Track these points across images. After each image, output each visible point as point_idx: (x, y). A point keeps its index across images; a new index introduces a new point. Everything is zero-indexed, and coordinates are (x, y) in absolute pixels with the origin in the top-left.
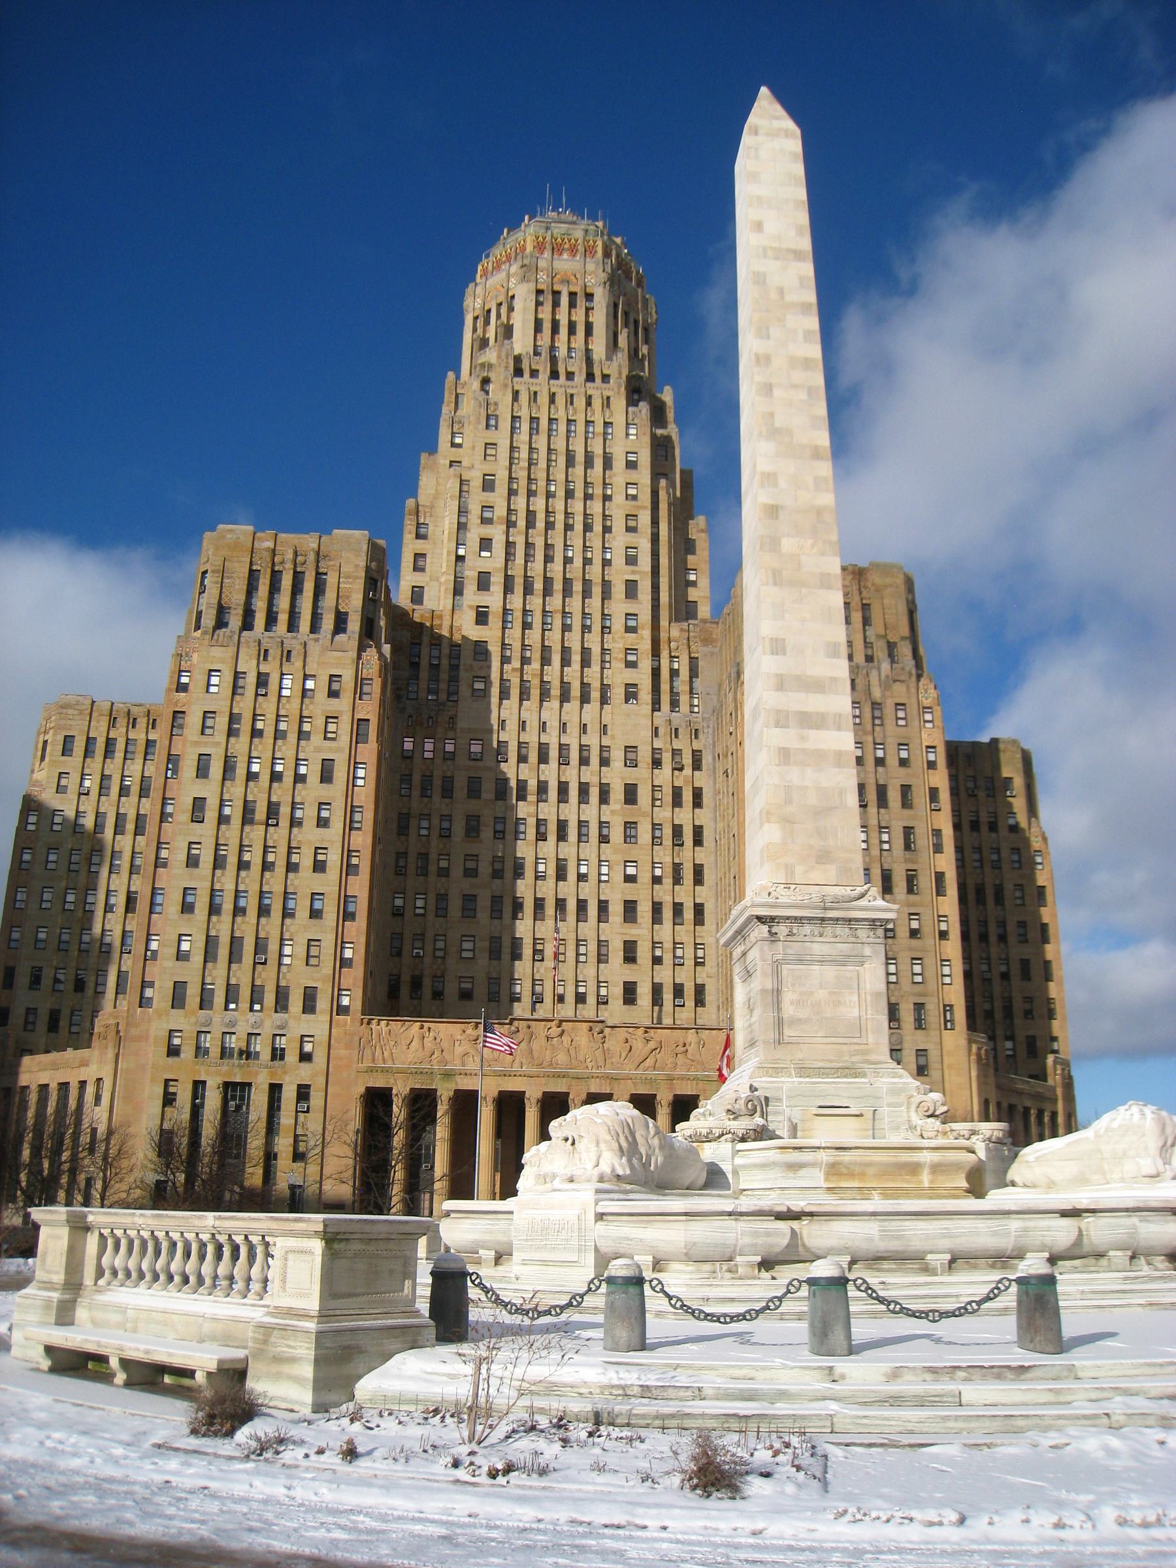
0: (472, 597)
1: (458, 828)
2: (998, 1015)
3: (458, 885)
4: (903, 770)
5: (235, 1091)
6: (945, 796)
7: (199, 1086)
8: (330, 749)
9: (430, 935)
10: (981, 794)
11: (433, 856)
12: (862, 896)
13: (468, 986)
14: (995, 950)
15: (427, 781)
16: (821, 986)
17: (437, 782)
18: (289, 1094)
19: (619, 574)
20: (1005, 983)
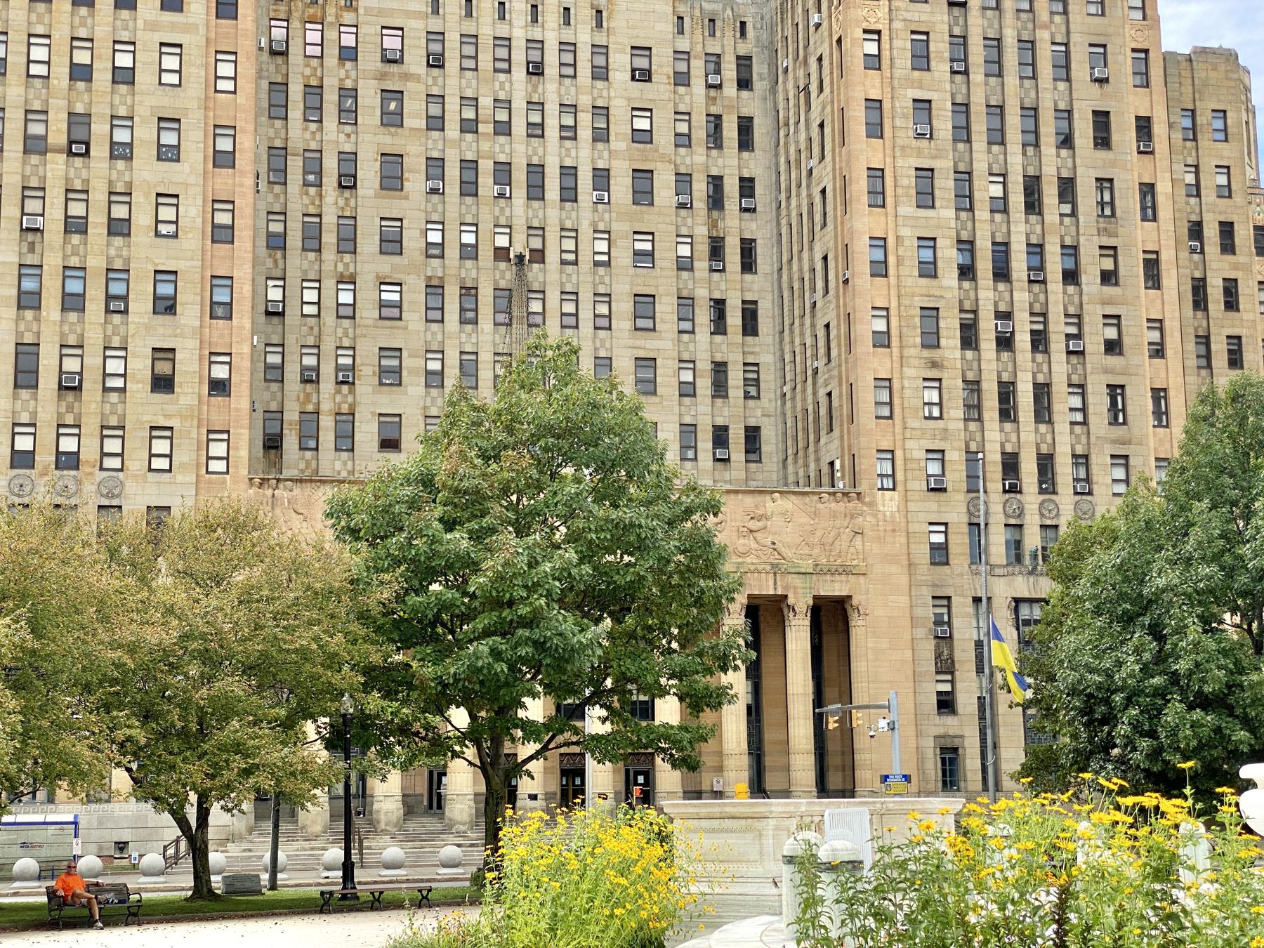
1: (368, 174)
8: (173, 27)
9: (328, 346)
15: (314, 91)
17: (331, 97)
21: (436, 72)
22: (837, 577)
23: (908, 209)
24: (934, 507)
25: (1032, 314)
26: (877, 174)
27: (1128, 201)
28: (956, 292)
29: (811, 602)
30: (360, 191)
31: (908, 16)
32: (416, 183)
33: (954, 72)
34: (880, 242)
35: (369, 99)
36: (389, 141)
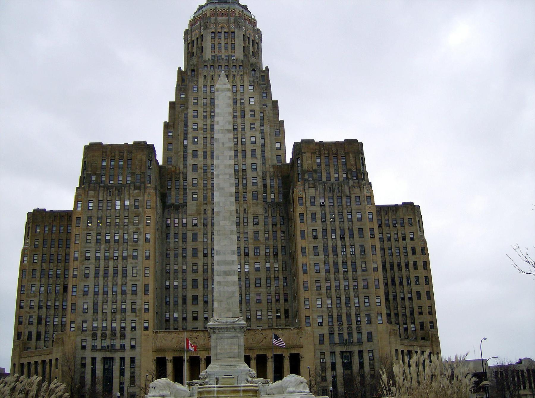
0: (190, 161)
2: (408, 314)
3: (190, 277)
4: (359, 223)
5: (108, 362)
6: (376, 231)
7: (94, 360)
10: (399, 226)
11: (180, 265)
12: (238, 321)
13: (196, 315)
14: (406, 289)
16: (227, 345)
18: (127, 361)
19: (249, 148)
20: (411, 301)
21: (205, 227)
22: (295, 349)
23: (312, 256)
24: (320, 330)
25: (344, 280)
26: (304, 248)
27: (369, 250)
28: (325, 276)
29: (289, 355)
30: (187, 258)
31: (311, 209)
32: (200, 255)
33: (322, 222)
34: (305, 265)
35: (189, 235)
36: (194, 244)
